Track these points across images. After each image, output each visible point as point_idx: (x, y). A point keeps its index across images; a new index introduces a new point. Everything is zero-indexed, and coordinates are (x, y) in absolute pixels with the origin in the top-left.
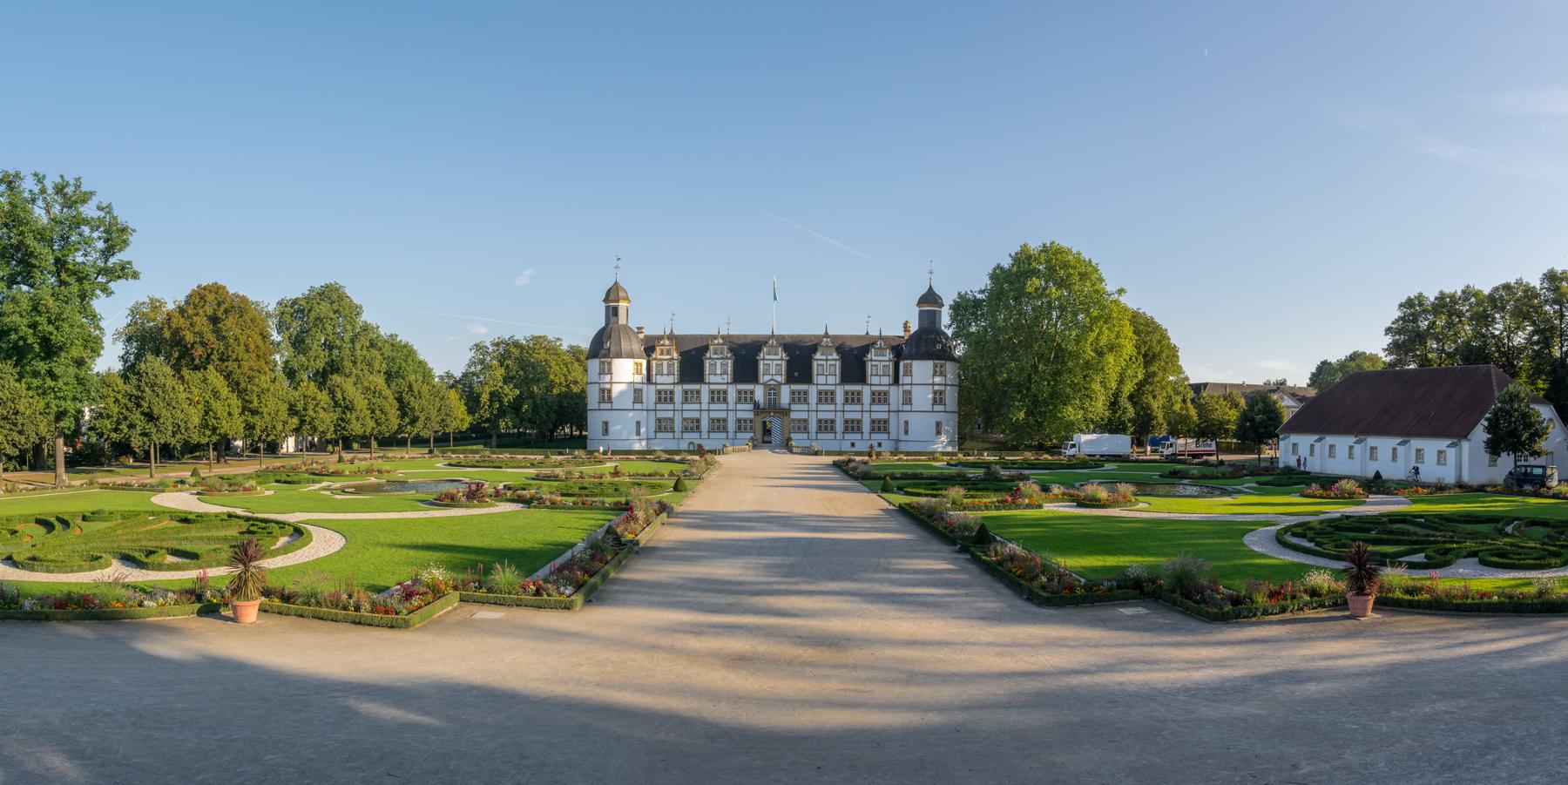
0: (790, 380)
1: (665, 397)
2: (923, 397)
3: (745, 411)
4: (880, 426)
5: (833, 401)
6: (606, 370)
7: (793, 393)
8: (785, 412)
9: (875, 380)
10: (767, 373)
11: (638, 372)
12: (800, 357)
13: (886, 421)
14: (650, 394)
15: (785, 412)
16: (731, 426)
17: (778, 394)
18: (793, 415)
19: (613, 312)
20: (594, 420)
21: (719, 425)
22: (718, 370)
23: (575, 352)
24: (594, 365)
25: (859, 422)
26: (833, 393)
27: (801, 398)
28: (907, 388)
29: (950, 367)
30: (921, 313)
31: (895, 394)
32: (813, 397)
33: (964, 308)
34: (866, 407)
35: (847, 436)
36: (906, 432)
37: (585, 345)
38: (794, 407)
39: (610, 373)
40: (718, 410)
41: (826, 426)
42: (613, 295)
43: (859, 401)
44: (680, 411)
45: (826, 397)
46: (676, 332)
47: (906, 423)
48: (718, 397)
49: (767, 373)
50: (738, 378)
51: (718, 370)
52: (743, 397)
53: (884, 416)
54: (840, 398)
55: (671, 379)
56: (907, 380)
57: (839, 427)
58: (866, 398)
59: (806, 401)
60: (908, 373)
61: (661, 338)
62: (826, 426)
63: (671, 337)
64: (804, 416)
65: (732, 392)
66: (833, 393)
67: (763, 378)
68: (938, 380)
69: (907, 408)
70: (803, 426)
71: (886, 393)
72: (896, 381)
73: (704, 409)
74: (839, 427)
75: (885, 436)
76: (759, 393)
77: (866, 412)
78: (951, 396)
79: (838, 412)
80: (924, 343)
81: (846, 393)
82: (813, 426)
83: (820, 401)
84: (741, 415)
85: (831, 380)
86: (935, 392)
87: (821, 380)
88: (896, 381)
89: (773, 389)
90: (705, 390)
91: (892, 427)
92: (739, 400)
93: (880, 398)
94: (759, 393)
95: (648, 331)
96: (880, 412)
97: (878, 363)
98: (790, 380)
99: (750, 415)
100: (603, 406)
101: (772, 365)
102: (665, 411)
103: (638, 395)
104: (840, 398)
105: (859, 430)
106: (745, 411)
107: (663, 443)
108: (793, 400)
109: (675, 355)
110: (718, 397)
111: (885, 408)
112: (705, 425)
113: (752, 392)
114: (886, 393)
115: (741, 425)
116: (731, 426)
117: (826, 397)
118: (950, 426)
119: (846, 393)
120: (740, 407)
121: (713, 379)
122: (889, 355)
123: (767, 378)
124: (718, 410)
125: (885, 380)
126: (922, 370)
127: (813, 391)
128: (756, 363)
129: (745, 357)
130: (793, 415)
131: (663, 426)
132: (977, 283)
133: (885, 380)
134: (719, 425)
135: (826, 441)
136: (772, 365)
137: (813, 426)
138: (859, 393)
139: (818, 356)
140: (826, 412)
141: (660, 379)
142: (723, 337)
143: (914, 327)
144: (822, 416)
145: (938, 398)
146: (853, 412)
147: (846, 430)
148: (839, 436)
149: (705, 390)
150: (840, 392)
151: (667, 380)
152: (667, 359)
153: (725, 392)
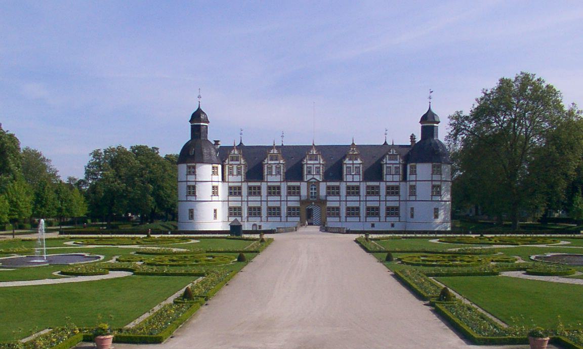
0: (327, 178)
2: (424, 190)
4: (393, 211)
5: (358, 194)
6: (192, 171)
7: (328, 188)
9: (389, 178)
10: (309, 173)
11: (214, 173)
13: (397, 208)
14: (223, 190)
16: (284, 211)
17: (317, 189)
18: (329, 204)
21: (274, 212)
24: (183, 168)
25: (378, 209)
26: (358, 188)
28: (413, 183)
30: (423, 128)
31: (404, 188)
32: (343, 191)
34: (383, 198)
35: (369, 219)
36: (412, 216)
37: (177, 151)
38: (329, 198)
39: (194, 173)
40: (274, 201)
41: (353, 212)
42: (197, 116)
43: (378, 194)
45: (353, 191)
46: (245, 144)
47: (412, 209)
48: (274, 191)
49: (309, 173)
50: (288, 177)
53: (396, 204)
54: (363, 191)
55: (239, 178)
56: (413, 177)
57: (363, 212)
58: (383, 191)
59: (338, 194)
60: (414, 172)
61: (231, 148)
62: (353, 212)
63: (241, 147)
64: (336, 204)
66: (358, 188)
67: (307, 178)
68: (435, 177)
69: (413, 198)
70: (335, 212)
71: (397, 187)
72: (405, 179)
73: (264, 201)
75: (397, 219)
79: (362, 202)
80: (425, 149)
81: (368, 187)
82: (343, 212)
83: (348, 194)
84: (290, 204)
85: (357, 178)
86: (433, 186)
87: (349, 178)
88: (405, 179)
91: (402, 212)
92: (289, 194)
93: (393, 191)
95: (221, 144)
96: (393, 201)
97: (391, 164)
98: (327, 178)
99: (297, 205)
100: (190, 198)
101: (314, 167)
104: (363, 191)
105: (378, 215)
106: (294, 201)
108: (328, 194)
109: (242, 161)
110: (274, 191)
111: (397, 198)
113: (299, 188)
114: (397, 187)
115: (291, 212)
117: (353, 191)
119: (368, 187)
120: (290, 198)
121: (270, 178)
123: (310, 177)
124: (274, 201)
125: (397, 178)
126: (423, 170)
128: (302, 165)
129: (294, 160)
130: (329, 204)
133: (397, 178)
134: (274, 212)
135: (353, 223)
136: (314, 167)
137: (343, 212)
138: (378, 187)
139: (347, 161)
140: (353, 201)
141: (231, 178)
142: (277, 147)
143: (418, 139)
144: (350, 204)
146: (373, 202)
147: (368, 215)
148: (363, 219)
149: (264, 186)
153: (279, 188)
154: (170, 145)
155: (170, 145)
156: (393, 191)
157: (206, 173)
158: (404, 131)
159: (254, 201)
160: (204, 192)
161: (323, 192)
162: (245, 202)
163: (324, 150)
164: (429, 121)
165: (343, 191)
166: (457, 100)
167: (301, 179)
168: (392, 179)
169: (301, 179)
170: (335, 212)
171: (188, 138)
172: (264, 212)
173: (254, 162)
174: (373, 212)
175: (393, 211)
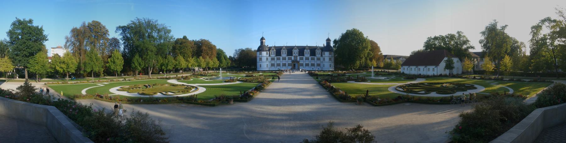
1: (273, 59)
3: (290, 62)
4: (318, 65)
6: (261, 54)
8: (298, 62)
11: (267, 54)
12: (301, 50)
14: (270, 59)
15: (299, 62)
16: (287, 65)
19: (262, 43)
20: (258, 64)
21: (284, 65)
22: (284, 54)
23: (255, 51)
24: (258, 53)
27: (302, 59)
29: (332, 53)
31: (322, 59)
32: (304, 59)
33: (335, 42)
37: (256, 49)
40: (284, 62)
41: (307, 65)
42: (262, 39)
44: (276, 62)
45: (307, 59)
48: (284, 59)
51: (284, 54)
52: (289, 59)
57: (310, 65)
62: (307, 65)
63: (275, 47)
65: (287, 57)
67: (294, 55)
72: (322, 56)
73: (281, 62)
74: (310, 65)
76: (293, 58)
77: (316, 62)
78: (333, 59)
79: (310, 62)
80: (327, 48)
82: (304, 65)
88: (322, 56)
89: (296, 57)
90: (281, 57)
93: (318, 59)
94: (293, 58)
96: (319, 62)
97: (318, 52)
98: (299, 55)
101: (295, 52)
102: (273, 62)
103: (267, 59)
106: (290, 62)
107: (273, 69)
110: (284, 59)
112: (281, 65)
115: (289, 65)
116: (287, 65)
117: (307, 59)
118: (333, 64)
122: (320, 51)
124: (284, 62)
126: (327, 54)
127: (304, 57)
129: (290, 50)
131: (273, 65)
132: (338, 37)
134: (284, 65)
135: (308, 68)
136: (295, 52)
137: (304, 65)
140: (307, 62)
143: (325, 45)
145: (330, 59)
146: (313, 62)
149: (281, 57)
150: (310, 58)
151: (273, 56)
152: (273, 52)
154: (254, 46)
155: (254, 46)
156: (318, 59)
157: (264, 53)
158: (322, 43)
159: (278, 62)
160: (264, 59)
161: (298, 59)
162: (276, 62)
163: (298, 47)
164: (328, 40)
165: (304, 59)
166: (336, 35)
167: (292, 55)
168: (318, 55)
169: (292, 55)
170: (302, 65)
171: (260, 45)
172: (281, 65)
173: (278, 51)
174: (313, 65)
175: (318, 65)
